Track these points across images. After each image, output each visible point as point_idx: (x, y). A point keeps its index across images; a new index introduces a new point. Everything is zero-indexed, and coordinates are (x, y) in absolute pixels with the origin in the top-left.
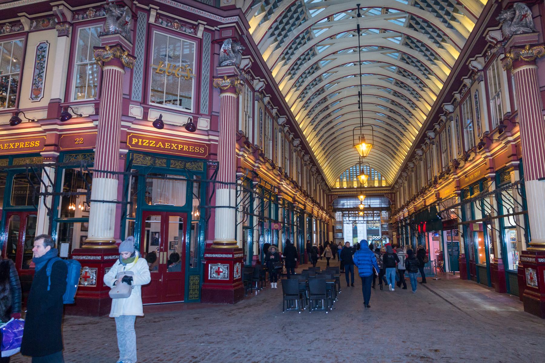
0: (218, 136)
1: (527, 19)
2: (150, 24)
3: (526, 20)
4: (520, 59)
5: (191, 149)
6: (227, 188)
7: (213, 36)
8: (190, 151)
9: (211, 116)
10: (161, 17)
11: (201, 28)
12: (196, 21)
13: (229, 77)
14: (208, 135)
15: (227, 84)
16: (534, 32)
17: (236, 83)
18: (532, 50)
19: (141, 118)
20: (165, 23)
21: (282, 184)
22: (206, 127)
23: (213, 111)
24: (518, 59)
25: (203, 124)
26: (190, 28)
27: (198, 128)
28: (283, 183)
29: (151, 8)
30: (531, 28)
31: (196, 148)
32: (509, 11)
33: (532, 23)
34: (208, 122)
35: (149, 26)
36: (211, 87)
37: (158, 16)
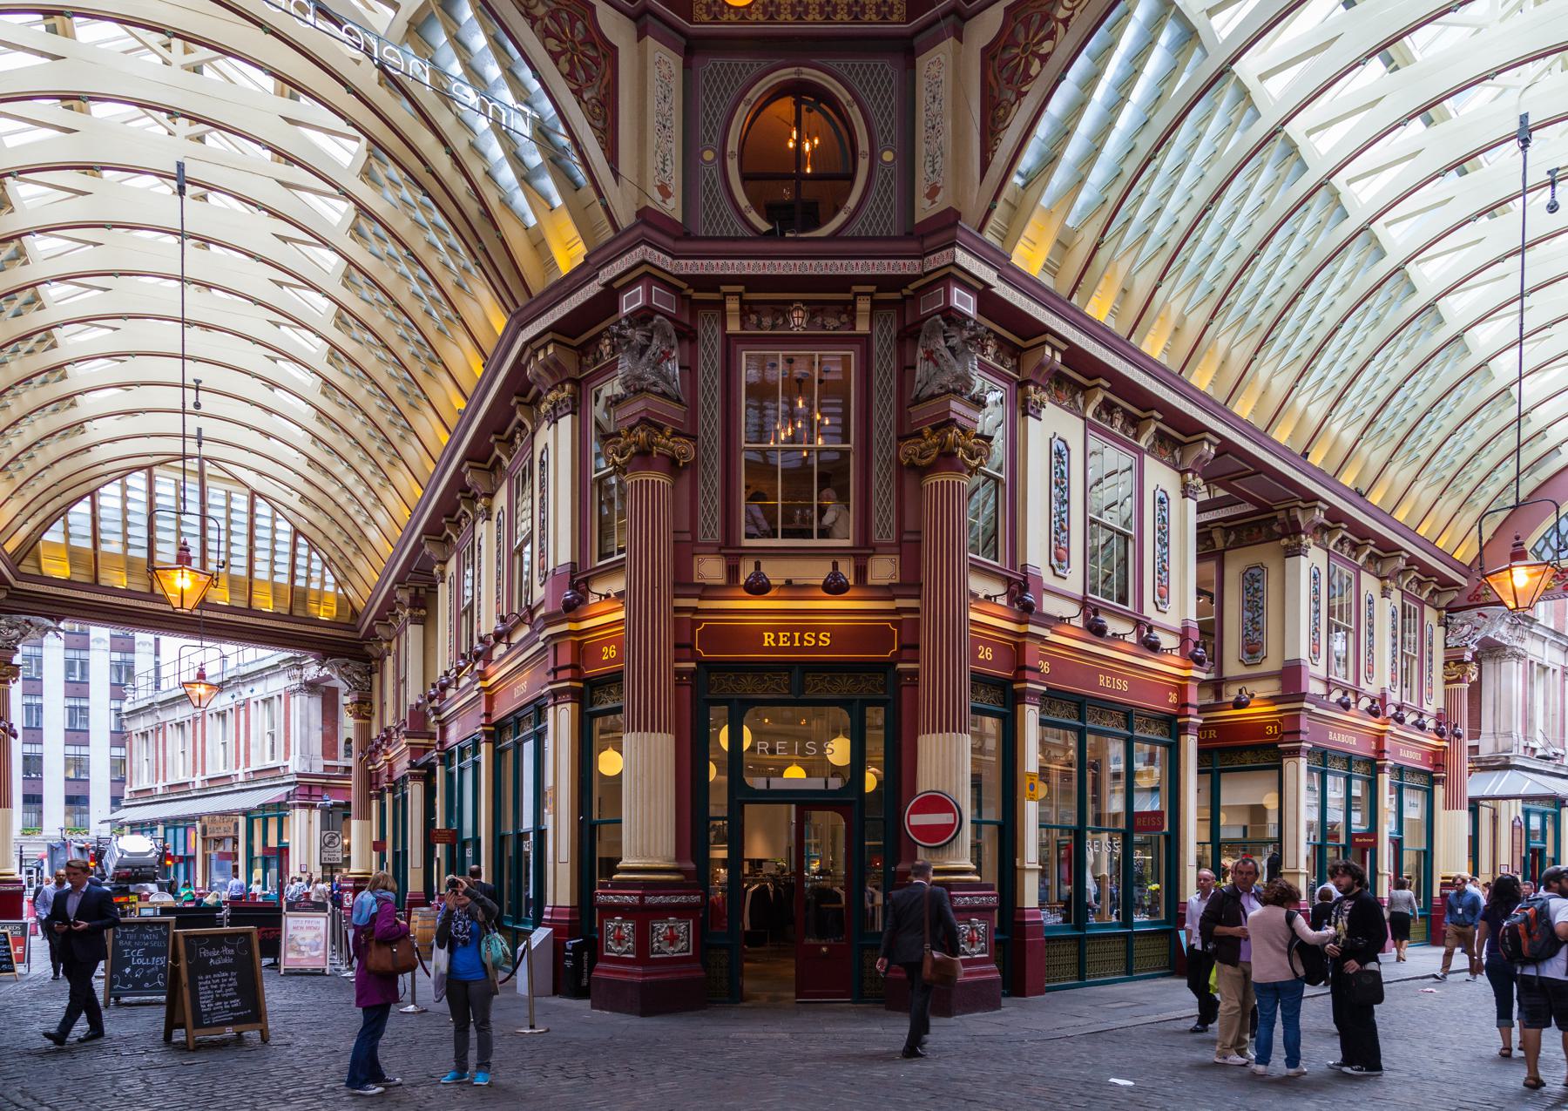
0: (918, 597)
7: (902, 316)
9: (900, 546)
10: (755, 307)
11: (863, 305)
12: (848, 291)
14: (892, 599)
19: (722, 582)
20: (767, 321)
25: (883, 570)
26: (838, 315)
29: (725, 294)
35: (728, 339)
37: (747, 309)
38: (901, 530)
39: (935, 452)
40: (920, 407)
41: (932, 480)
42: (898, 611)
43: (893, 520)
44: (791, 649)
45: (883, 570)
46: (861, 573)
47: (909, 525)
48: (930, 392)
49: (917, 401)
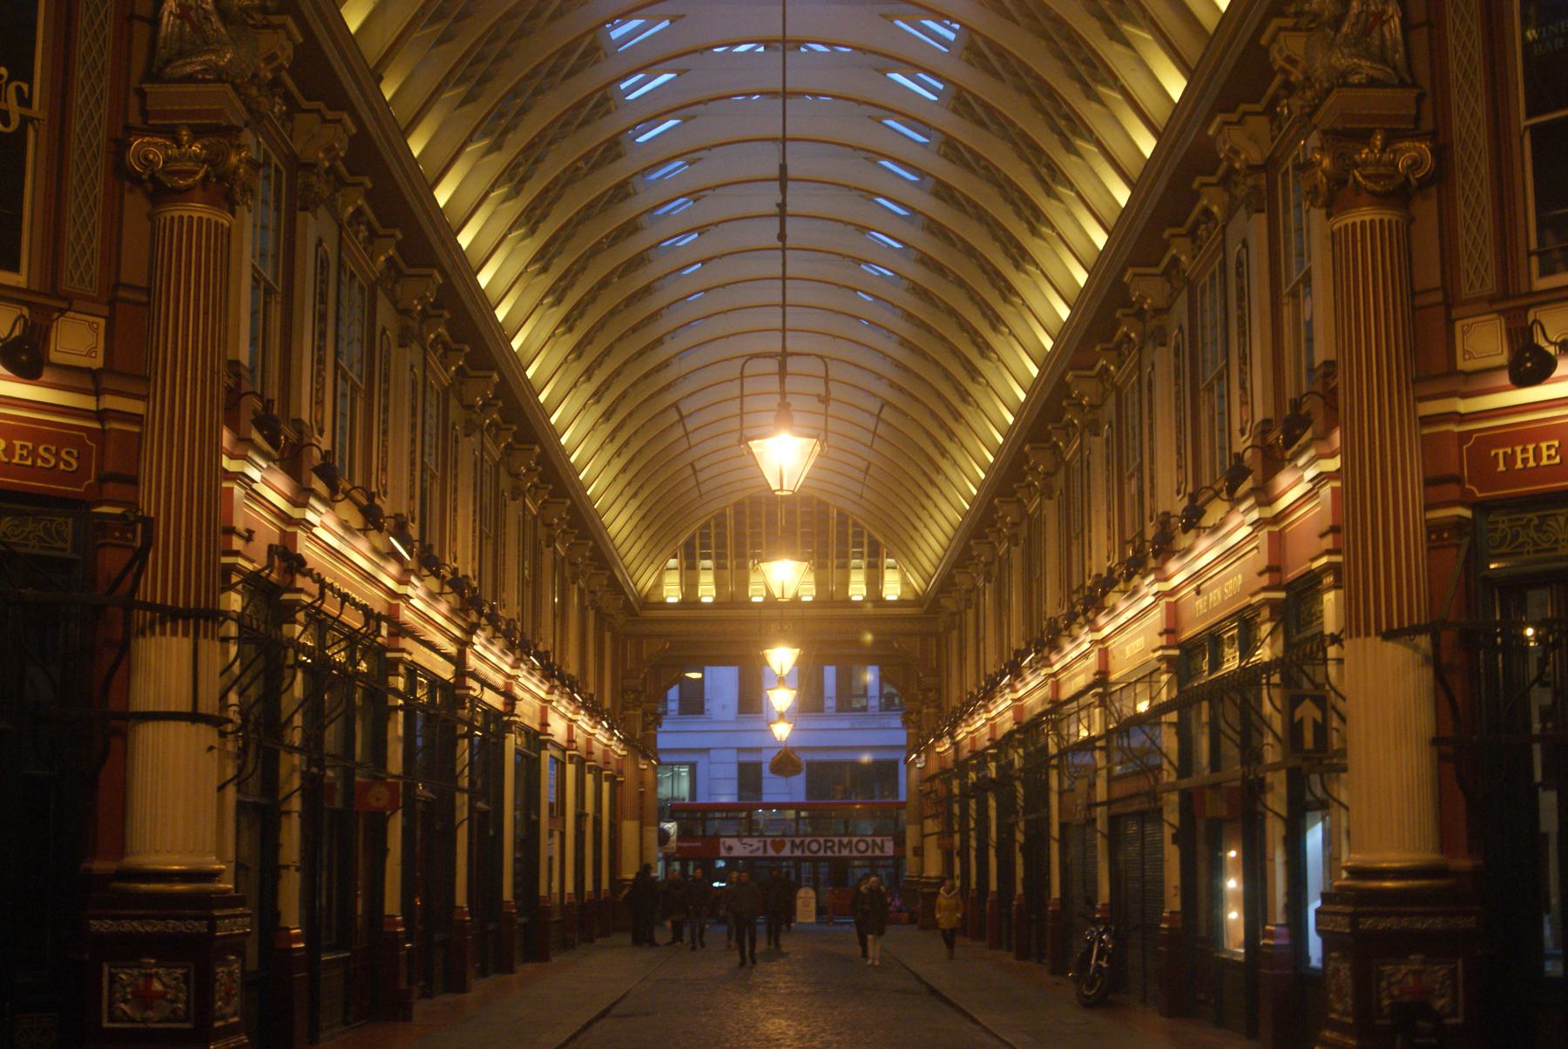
1: (1386, 28)
3: (1383, 35)
4: (1351, 177)
5: (18, 452)
6: (186, 634)
8: (16, 460)
13: (198, 133)
15: (189, 166)
16: (1402, 84)
17: (234, 159)
18: (1395, 152)
21: (406, 597)
22: (88, 355)
23: (124, 278)
24: (1346, 182)
27: (55, 357)
28: (409, 590)
30: (1394, 68)
31: (41, 450)
33: (1401, 49)
34: (96, 330)
36: (120, 171)
42: (101, 415)
47: (133, 271)
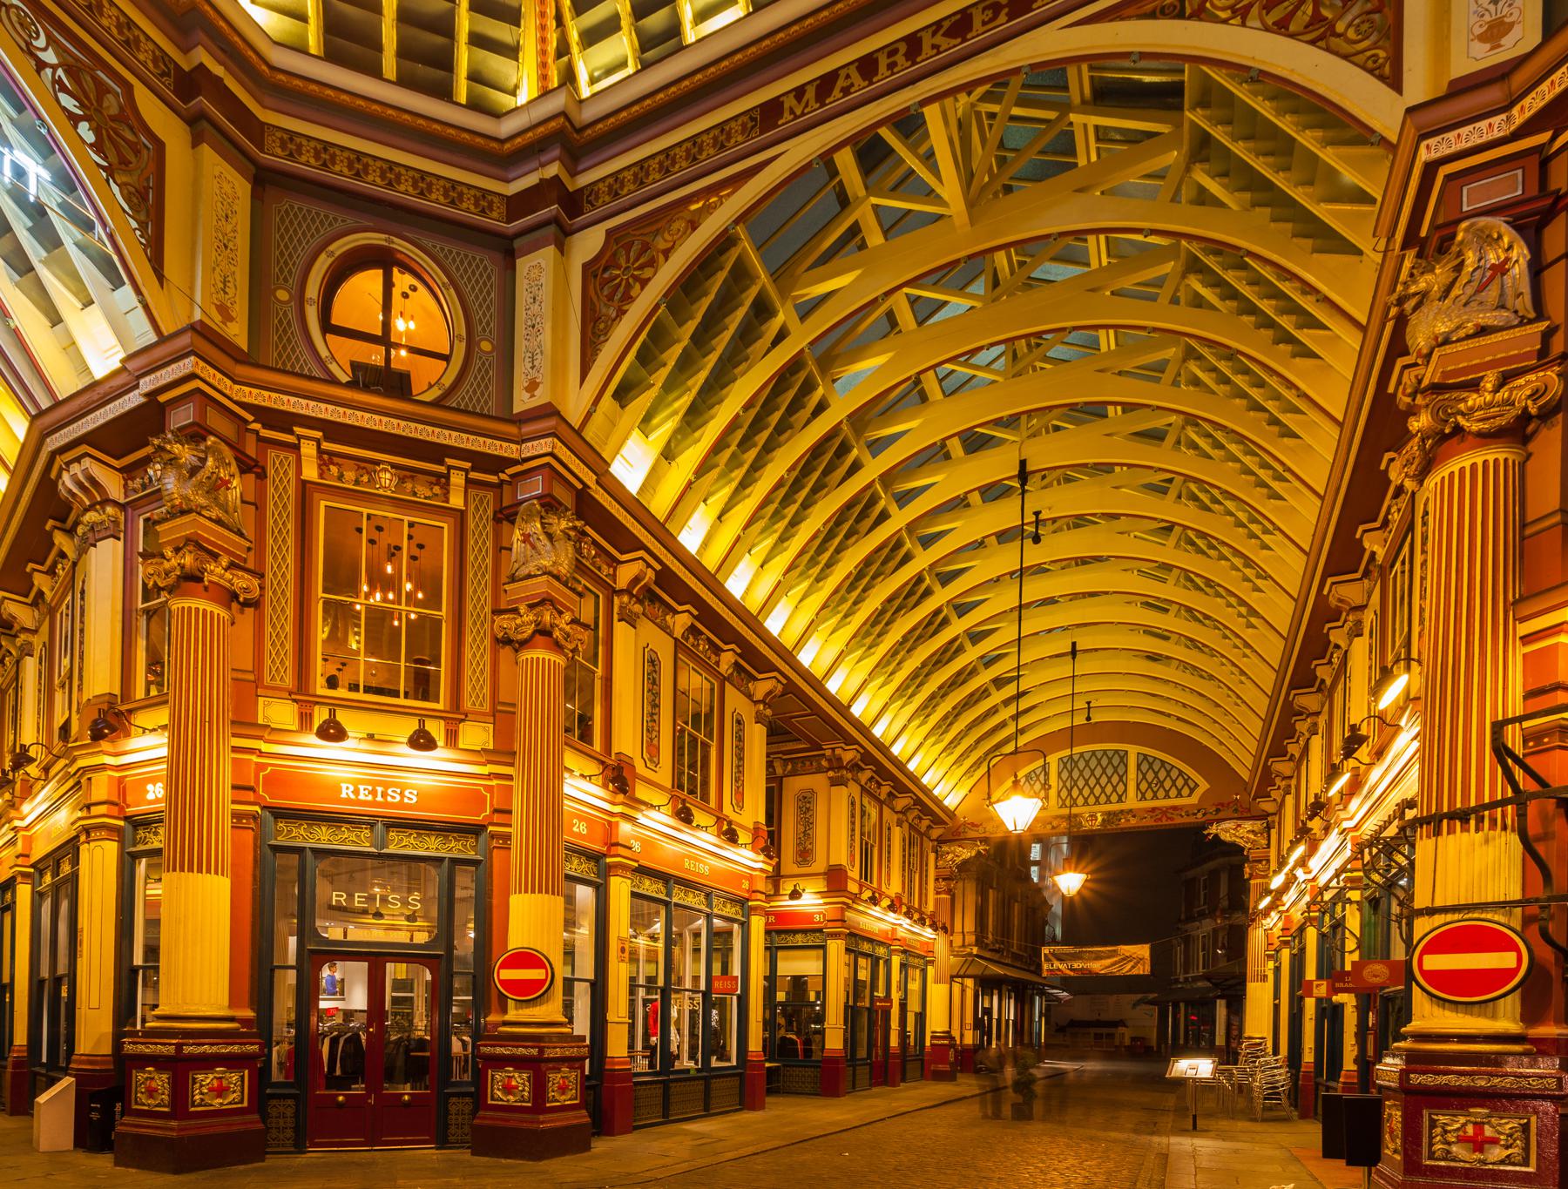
2: (304, 482)
10: (336, 460)
20: (350, 475)
25: (476, 735)
32: (1438, 263)
38: (494, 699)
39: (530, 630)
40: (516, 585)
41: (527, 655)
42: (490, 776)
43: (487, 690)
44: (374, 804)
45: (476, 735)
46: (452, 739)
48: (527, 572)
49: (513, 579)
